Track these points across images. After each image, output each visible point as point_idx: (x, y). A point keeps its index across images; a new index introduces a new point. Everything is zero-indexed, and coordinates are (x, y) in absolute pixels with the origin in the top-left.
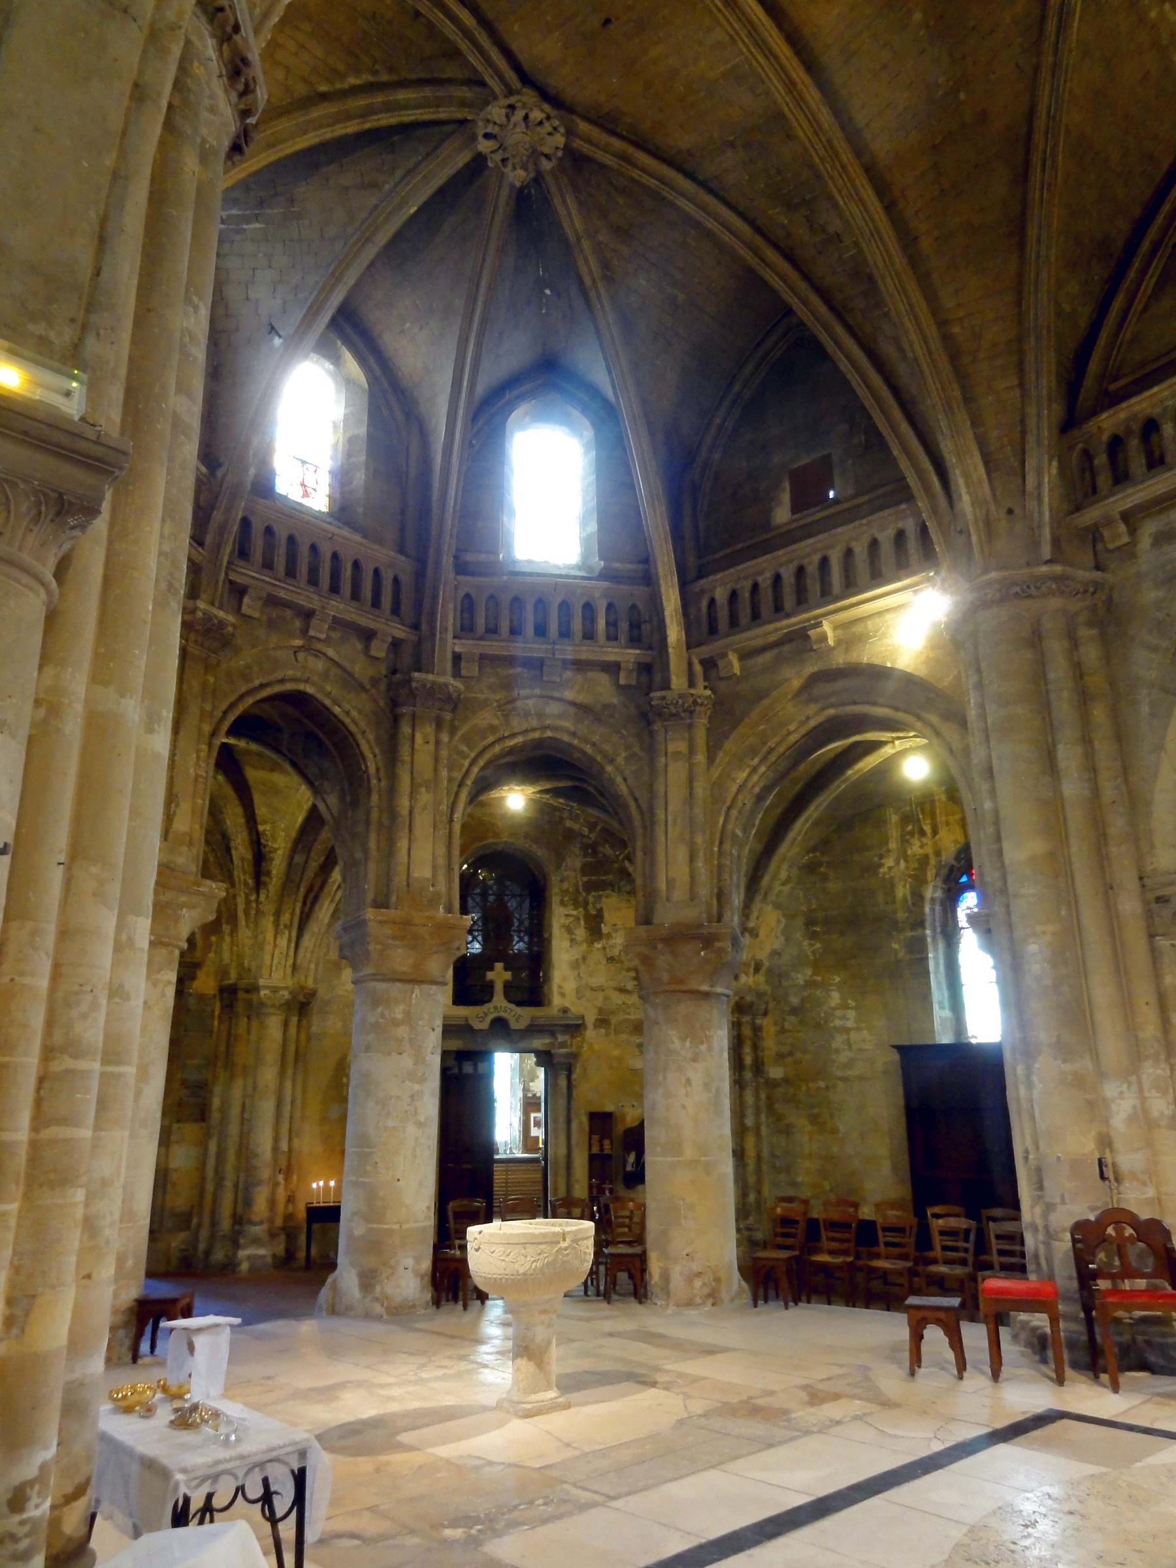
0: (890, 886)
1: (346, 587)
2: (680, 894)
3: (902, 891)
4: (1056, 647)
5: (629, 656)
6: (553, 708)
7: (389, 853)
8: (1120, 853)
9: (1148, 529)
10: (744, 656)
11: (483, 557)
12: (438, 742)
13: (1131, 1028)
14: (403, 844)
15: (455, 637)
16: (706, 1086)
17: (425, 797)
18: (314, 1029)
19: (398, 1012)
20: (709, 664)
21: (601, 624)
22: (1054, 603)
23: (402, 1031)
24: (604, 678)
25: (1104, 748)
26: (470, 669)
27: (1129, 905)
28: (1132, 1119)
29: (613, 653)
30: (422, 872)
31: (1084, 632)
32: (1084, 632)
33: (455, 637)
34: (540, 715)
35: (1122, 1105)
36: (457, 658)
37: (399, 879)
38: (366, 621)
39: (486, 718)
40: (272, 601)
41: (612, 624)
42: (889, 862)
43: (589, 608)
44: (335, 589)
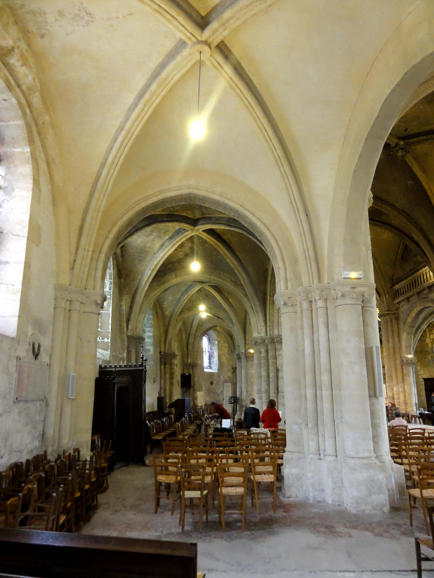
0: (428, 346)
3: (430, 346)
4: (389, 324)
8: (397, 354)
9: (401, 305)
13: (397, 379)
22: (388, 317)
27: (398, 362)
28: (396, 391)
31: (394, 321)
32: (394, 321)
35: (395, 389)
42: (427, 339)
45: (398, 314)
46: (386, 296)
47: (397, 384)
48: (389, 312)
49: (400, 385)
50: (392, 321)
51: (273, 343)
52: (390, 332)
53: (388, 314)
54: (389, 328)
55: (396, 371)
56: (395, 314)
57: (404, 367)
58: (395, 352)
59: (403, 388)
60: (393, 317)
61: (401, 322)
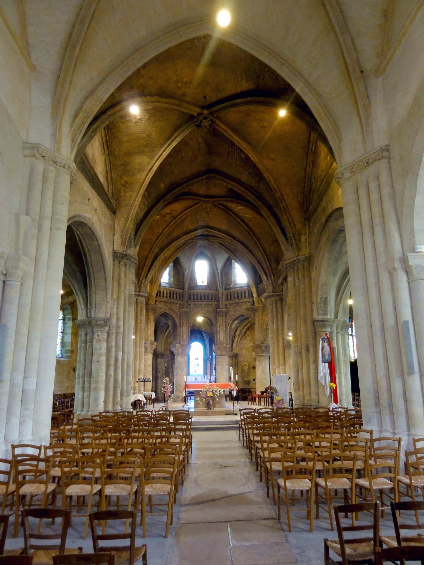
1: (206, 299)
2: (258, 339)
5: (251, 300)
6: (242, 310)
7: (217, 336)
10: (265, 298)
11: (229, 287)
12: (223, 319)
13: (279, 362)
14: (218, 335)
15: (225, 301)
16: (262, 370)
17: (221, 328)
18: (239, 360)
19: (219, 360)
20: (260, 300)
21: (247, 295)
22: (273, 299)
23: (219, 363)
24: (249, 303)
25: (279, 320)
26: (228, 306)
27: (281, 344)
29: (248, 300)
30: (221, 339)
32: (278, 302)
33: (225, 301)
34: (240, 311)
36: (226, 304)
37: (218, 341)
38: (210, 303)
39: (232, 313)
40: (195, 304)
41: (249, 294)
43: (245, 292)
44: (205, 299)
45: (282, 295)
46: (271, 277)
47: (279, 367)
48: (274, 294)
49: (281, 367)
50: (276, 303)
51: (90, 325)
52: (275, 315)
53: (273, 295)
54: (274, 309)
55: (278, 353)
56: (279, 295)
57: (286, 349)
58: (278, 333)
59: (284, 370)
60: (277, 298)
61: (284, 303)
